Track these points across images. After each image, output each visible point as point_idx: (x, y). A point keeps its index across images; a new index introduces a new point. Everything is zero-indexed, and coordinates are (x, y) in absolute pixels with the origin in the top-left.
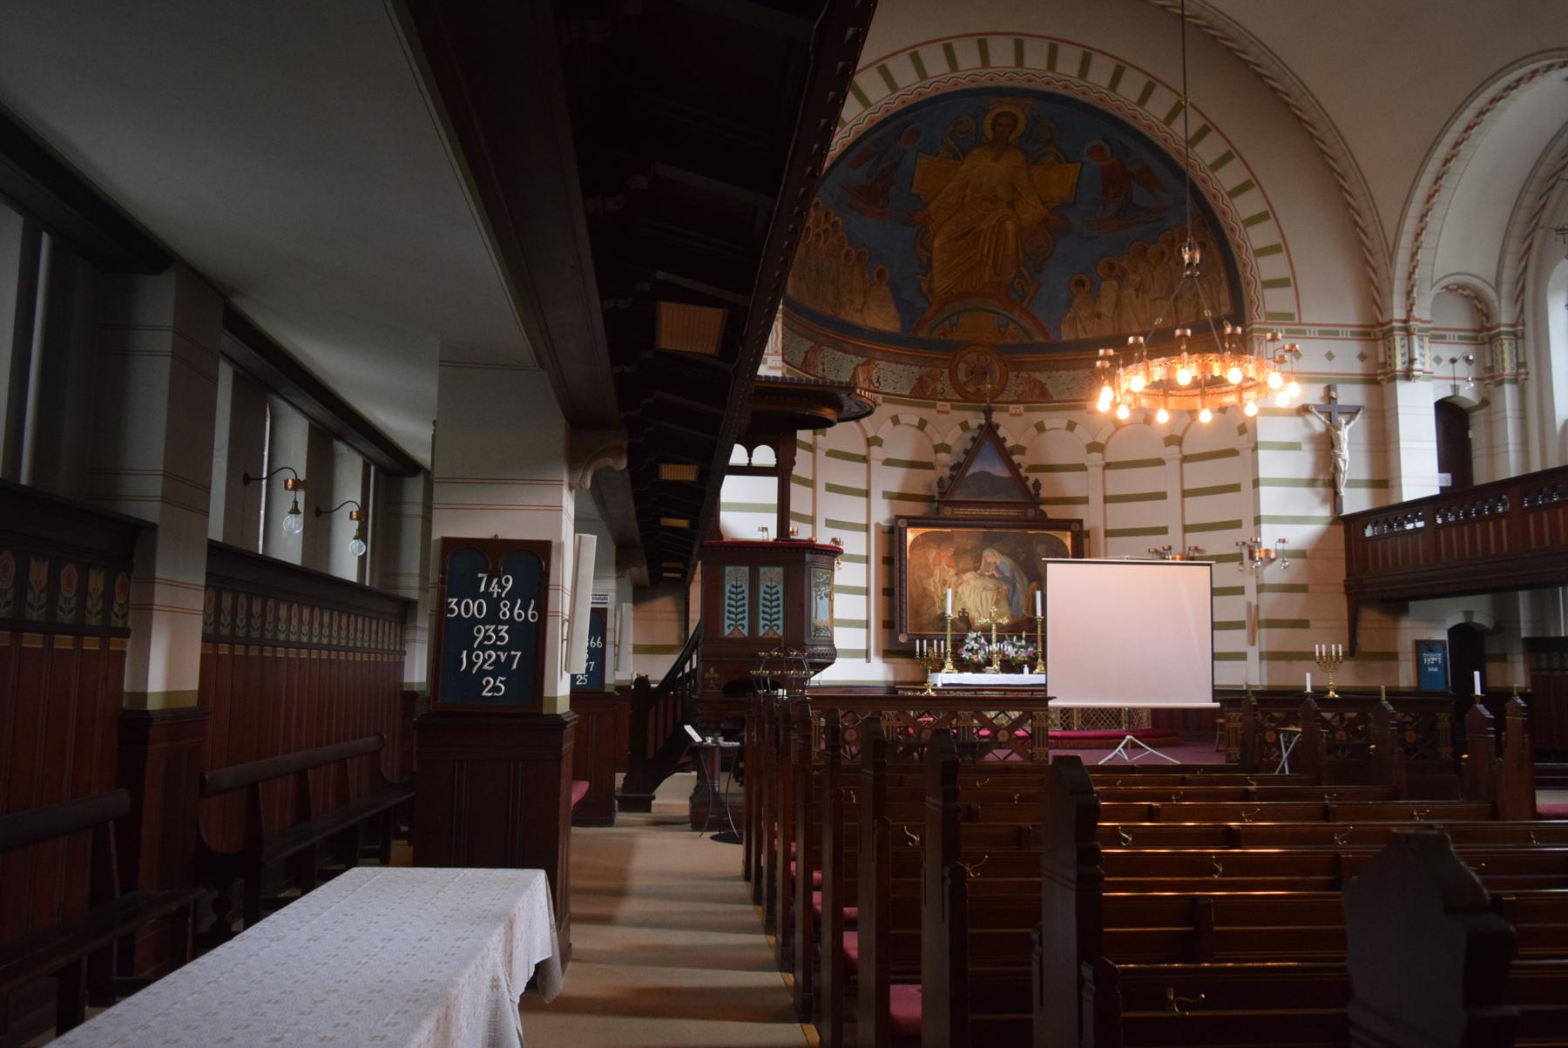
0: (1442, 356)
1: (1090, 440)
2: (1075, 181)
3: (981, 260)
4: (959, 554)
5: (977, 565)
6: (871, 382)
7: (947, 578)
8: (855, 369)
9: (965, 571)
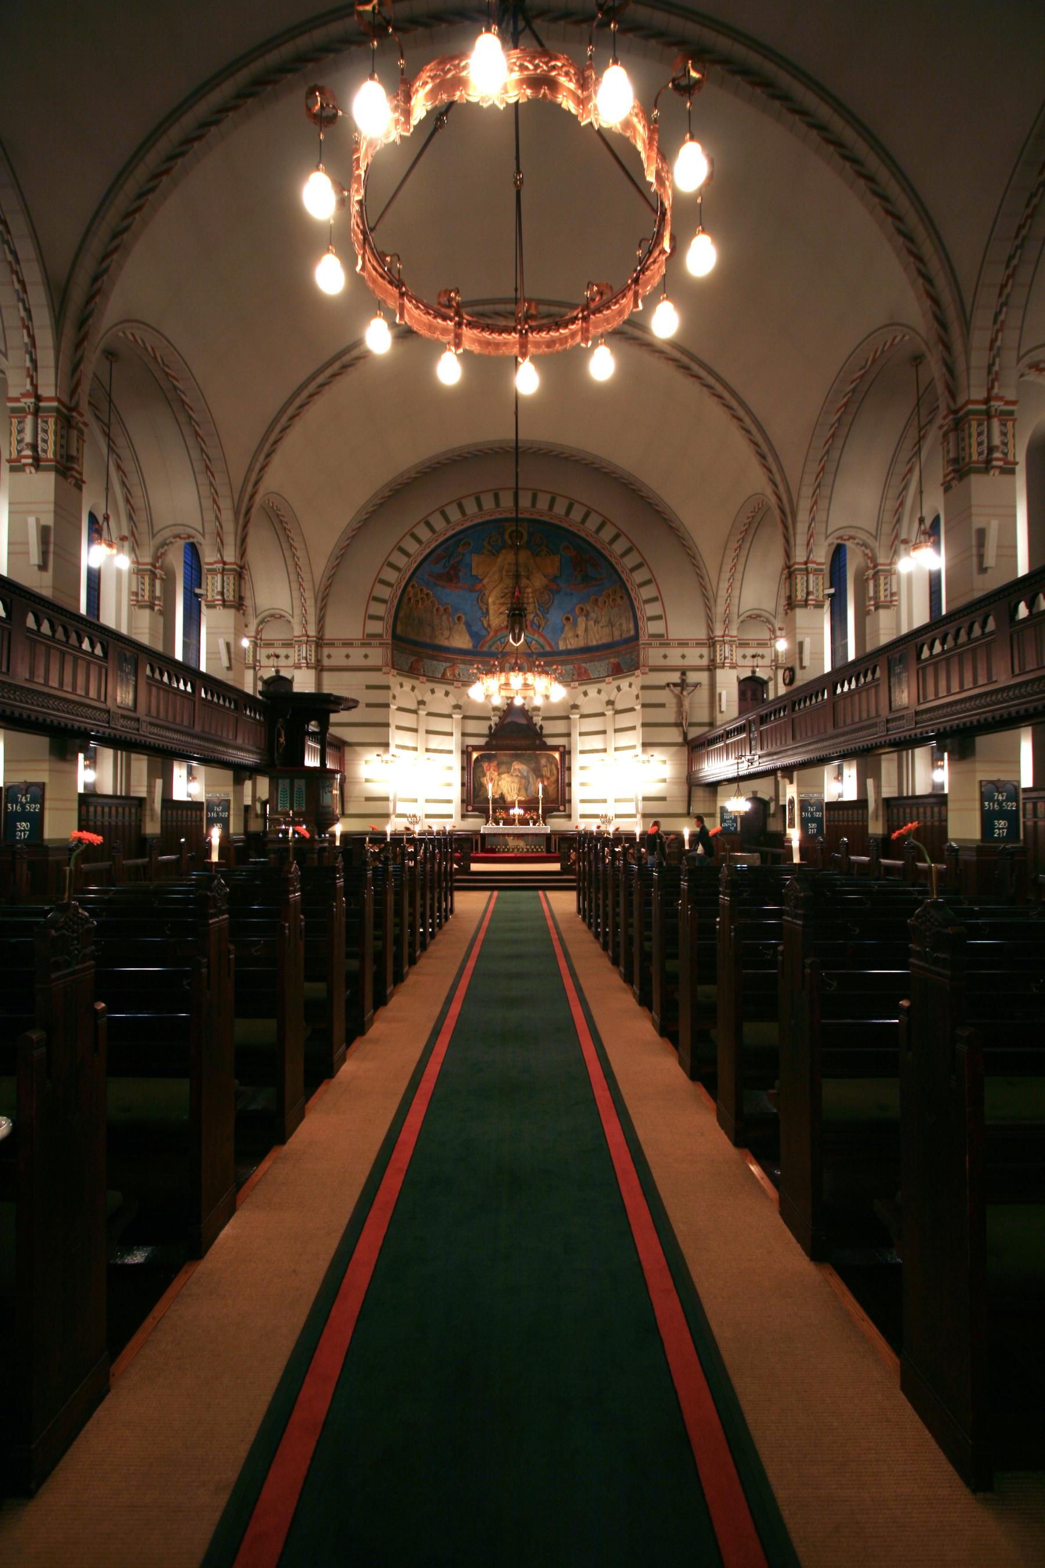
0: (747, 654)
4: (498, 766)
6: (454, 676)
8: (445, 670)
9: (503, 773)
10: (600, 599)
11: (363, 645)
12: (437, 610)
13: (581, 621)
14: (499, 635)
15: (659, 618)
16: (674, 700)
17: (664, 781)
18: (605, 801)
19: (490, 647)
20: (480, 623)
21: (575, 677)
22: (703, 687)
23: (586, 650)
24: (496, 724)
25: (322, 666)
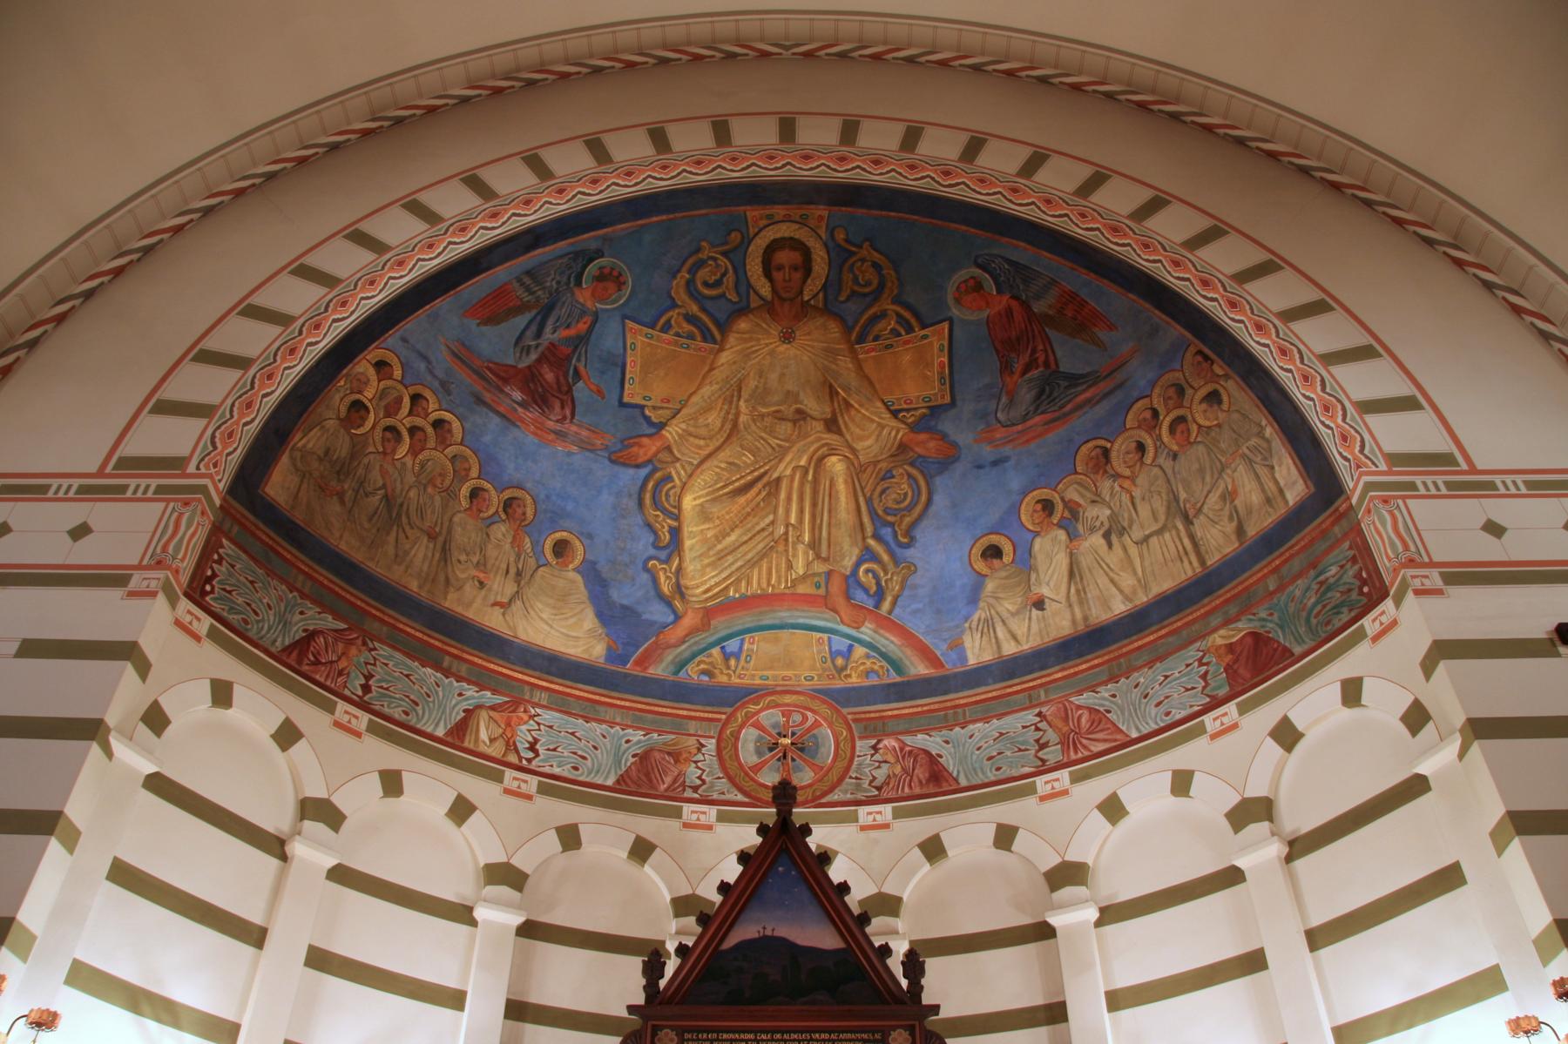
1: (1054, 860)
2: (946, 360)
3: (786, 533)
6: (511, 746)
8: (469, 713)
10: (1120, 449)
12: (475, 493)
13: (1051, 551)
14: (721, 626)
19: (681, 665)
20: (645, 576)
21: (1053, 754)
24: (682, 950)
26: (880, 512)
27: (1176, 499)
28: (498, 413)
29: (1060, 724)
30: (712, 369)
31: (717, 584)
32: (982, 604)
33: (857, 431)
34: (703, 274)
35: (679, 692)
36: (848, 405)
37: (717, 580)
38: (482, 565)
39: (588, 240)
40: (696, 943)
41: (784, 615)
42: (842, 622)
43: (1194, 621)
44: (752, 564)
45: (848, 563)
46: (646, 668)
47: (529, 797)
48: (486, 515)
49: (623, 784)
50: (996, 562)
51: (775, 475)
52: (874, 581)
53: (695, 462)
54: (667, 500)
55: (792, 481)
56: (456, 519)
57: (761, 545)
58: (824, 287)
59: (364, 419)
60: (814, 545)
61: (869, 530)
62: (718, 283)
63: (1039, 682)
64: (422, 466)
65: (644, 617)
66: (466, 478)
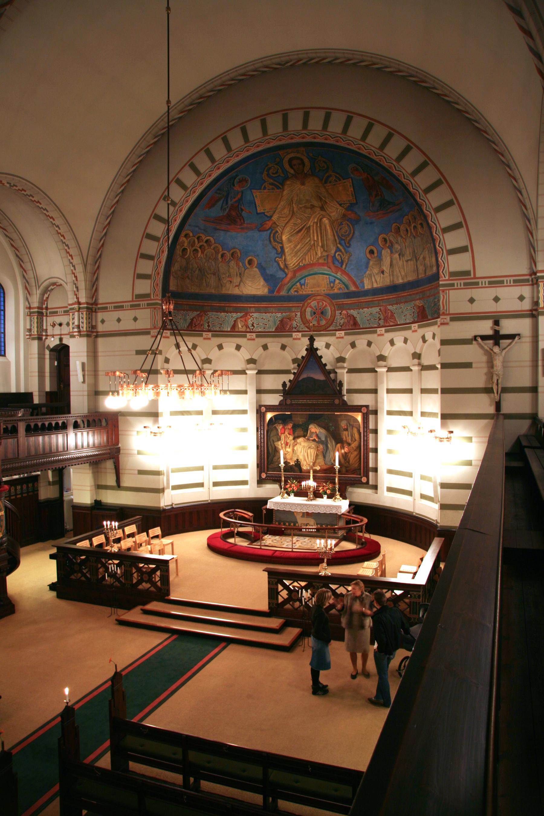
1: (378, 354)
2: (352, 189)
3: (314, 243)
4: (295, 427)
5: (305, 433)
6: (247, 327)
7: (288, 441)
8: (235, 321)
9: (299, 437)
10: (402, 228)
11: (134, 307)
12: (223, 256)
14: (299, 275)
15: (463, 249)
16: (484, 358)
17: (469, 463)
18: (410, 475)
19: (289, 290)
20: (276, 264)
21: (382, 322)
22: (523, 340)
23: (392, 289)
24: (290, 381)
25: (97, 332)
26: (340, 236)
27: (415, 251)
28: (222, 230)
29: (384, 314)
30: (282, 197)
31: (296, 262)
32: (369, 269)
33: (330, 210)
34: (271, 171)
35: (289, 299)
36: (326, 203)
37: (296, 261)
38: (230, 276)
39: (233, 173)
40: (297, 371)
41: (316, 269)
42: (332, 272)
43: (414, 294)
44: (306, 254)
45: (333, 252)
46: (280, 293)
47: (254, 339)
48: (227, 260)
49: (277, 330)
50: (372, 255)
51: (308, 225)
52: (340, 258)
53: (284, 225)
54: (278, 238)
55: (313, 227)
56: (220, 265)
57: (307, 248)
58: (310, 168)
59: (187, 252)
60: (323, 246)
61: (338, 241)
62: (277, 173)
63: (381, 298)
64: (206, 255)
65: (277, 276)
66: (219, 252)
